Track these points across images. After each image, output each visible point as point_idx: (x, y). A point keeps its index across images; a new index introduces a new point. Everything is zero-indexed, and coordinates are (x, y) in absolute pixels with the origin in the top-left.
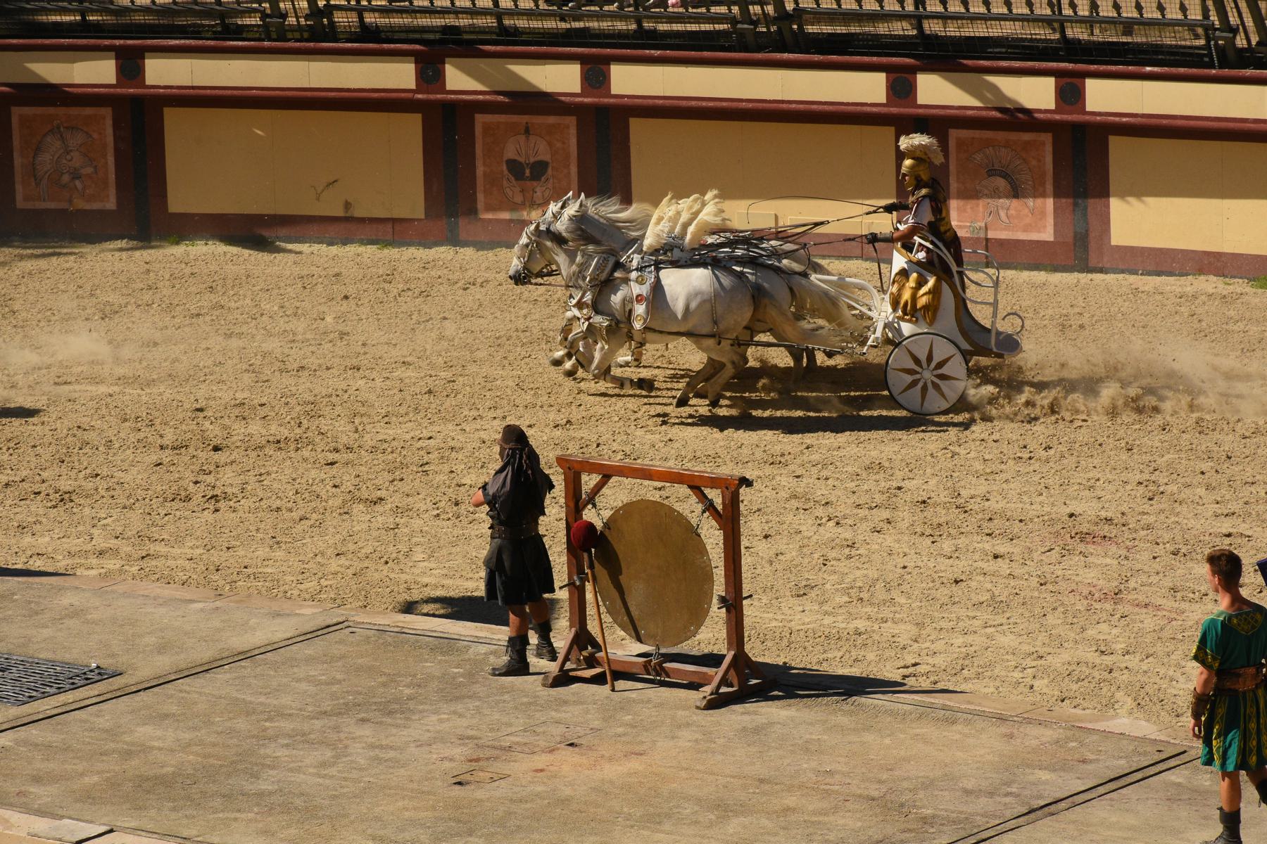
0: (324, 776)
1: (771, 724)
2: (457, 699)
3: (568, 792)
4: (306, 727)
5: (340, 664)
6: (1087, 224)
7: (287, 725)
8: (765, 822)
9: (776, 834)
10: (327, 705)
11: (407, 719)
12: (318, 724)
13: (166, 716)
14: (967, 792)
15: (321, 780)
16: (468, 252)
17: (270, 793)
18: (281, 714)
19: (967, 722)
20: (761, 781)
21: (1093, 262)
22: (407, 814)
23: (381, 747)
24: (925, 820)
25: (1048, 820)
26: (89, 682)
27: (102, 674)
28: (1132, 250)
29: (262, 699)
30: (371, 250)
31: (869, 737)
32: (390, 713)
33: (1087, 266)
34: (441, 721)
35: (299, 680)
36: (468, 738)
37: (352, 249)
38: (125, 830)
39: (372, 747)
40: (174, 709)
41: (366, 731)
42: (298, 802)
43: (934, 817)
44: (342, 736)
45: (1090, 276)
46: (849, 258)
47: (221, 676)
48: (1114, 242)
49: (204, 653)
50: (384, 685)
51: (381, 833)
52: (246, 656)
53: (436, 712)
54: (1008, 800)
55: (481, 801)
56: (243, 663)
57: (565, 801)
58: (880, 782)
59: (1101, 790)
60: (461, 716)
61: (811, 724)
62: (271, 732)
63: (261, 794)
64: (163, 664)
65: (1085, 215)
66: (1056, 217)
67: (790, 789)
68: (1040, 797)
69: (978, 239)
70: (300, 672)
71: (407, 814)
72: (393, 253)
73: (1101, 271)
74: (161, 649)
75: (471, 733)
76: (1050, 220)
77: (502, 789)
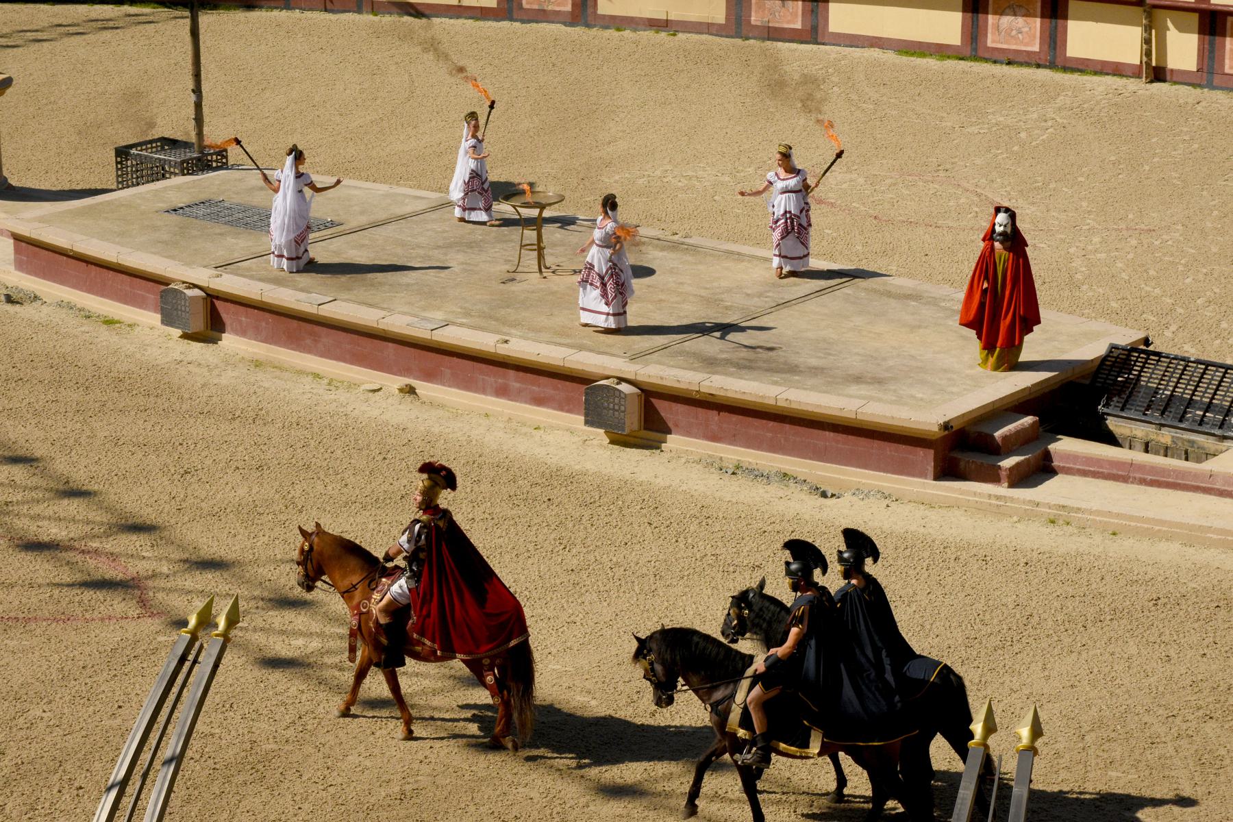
0: (438, 277)
1: (654, 259)
2: (506, 241)
3: (555, 288)
4: (431, 253)
5: (448, 223)
6: (817, 20)
7: (421, 252)
8: (650, 306)
9: (655, 312)
10: (440, 243)
11: (480, 251)
12: (437, 251)
13: (363, 246)
14: (748, 295)
15: (436, 279)
16: (517, 24)
17: (413, 285)
18: (418, 246)
19: (749, 261)
20: (649, 286)
21: (819, 41)
22: (478, 297)
23: (466, 264)
24: (727, 308)
25: (786, 310)
26: (327, 227)
27: (333, 224)
28: (839, 35)
29: (409, 239)
30: (470, 21)
31: (701, 267)
32: (472, 247)
33: (816, 39)
34: (496, 252)
35: (428, 230)
36: (510, 261)
37: (461, 21)
38: (340, 300)
39: (462, 263)
40: (367, 242)
41: (461, 257)
42: (426, 289)
43: (731, 306)
44: (448, 258)
45: (818, 46)
46: (702, 33)
47: (391, 227)
48: (830, 31)
49: (382, 216)
50: (469, 234)
51: (466, 305)
52: (404, 217)
53: (494, 248)
54: (767, 299)
55: (514, 291)
56: (401, 221)
57: (553, 293)
58: (706, 288)
59: (812, 296)
60: (506, 250)
61: (674, 259)
62: (413, 255)
63: (408, 285)
64: (363, 220)
65: (817, 17)
66: (802, 17)
67: (662, 291)
68: (783, 298)
69: (764, 27)
70: (429, 226)
71: (478, 297)
72: (481, 23)
73: (823, 44)
74: (362, 213)
75: (511, 259)
76: (800, 19)
77: (523, 286)
